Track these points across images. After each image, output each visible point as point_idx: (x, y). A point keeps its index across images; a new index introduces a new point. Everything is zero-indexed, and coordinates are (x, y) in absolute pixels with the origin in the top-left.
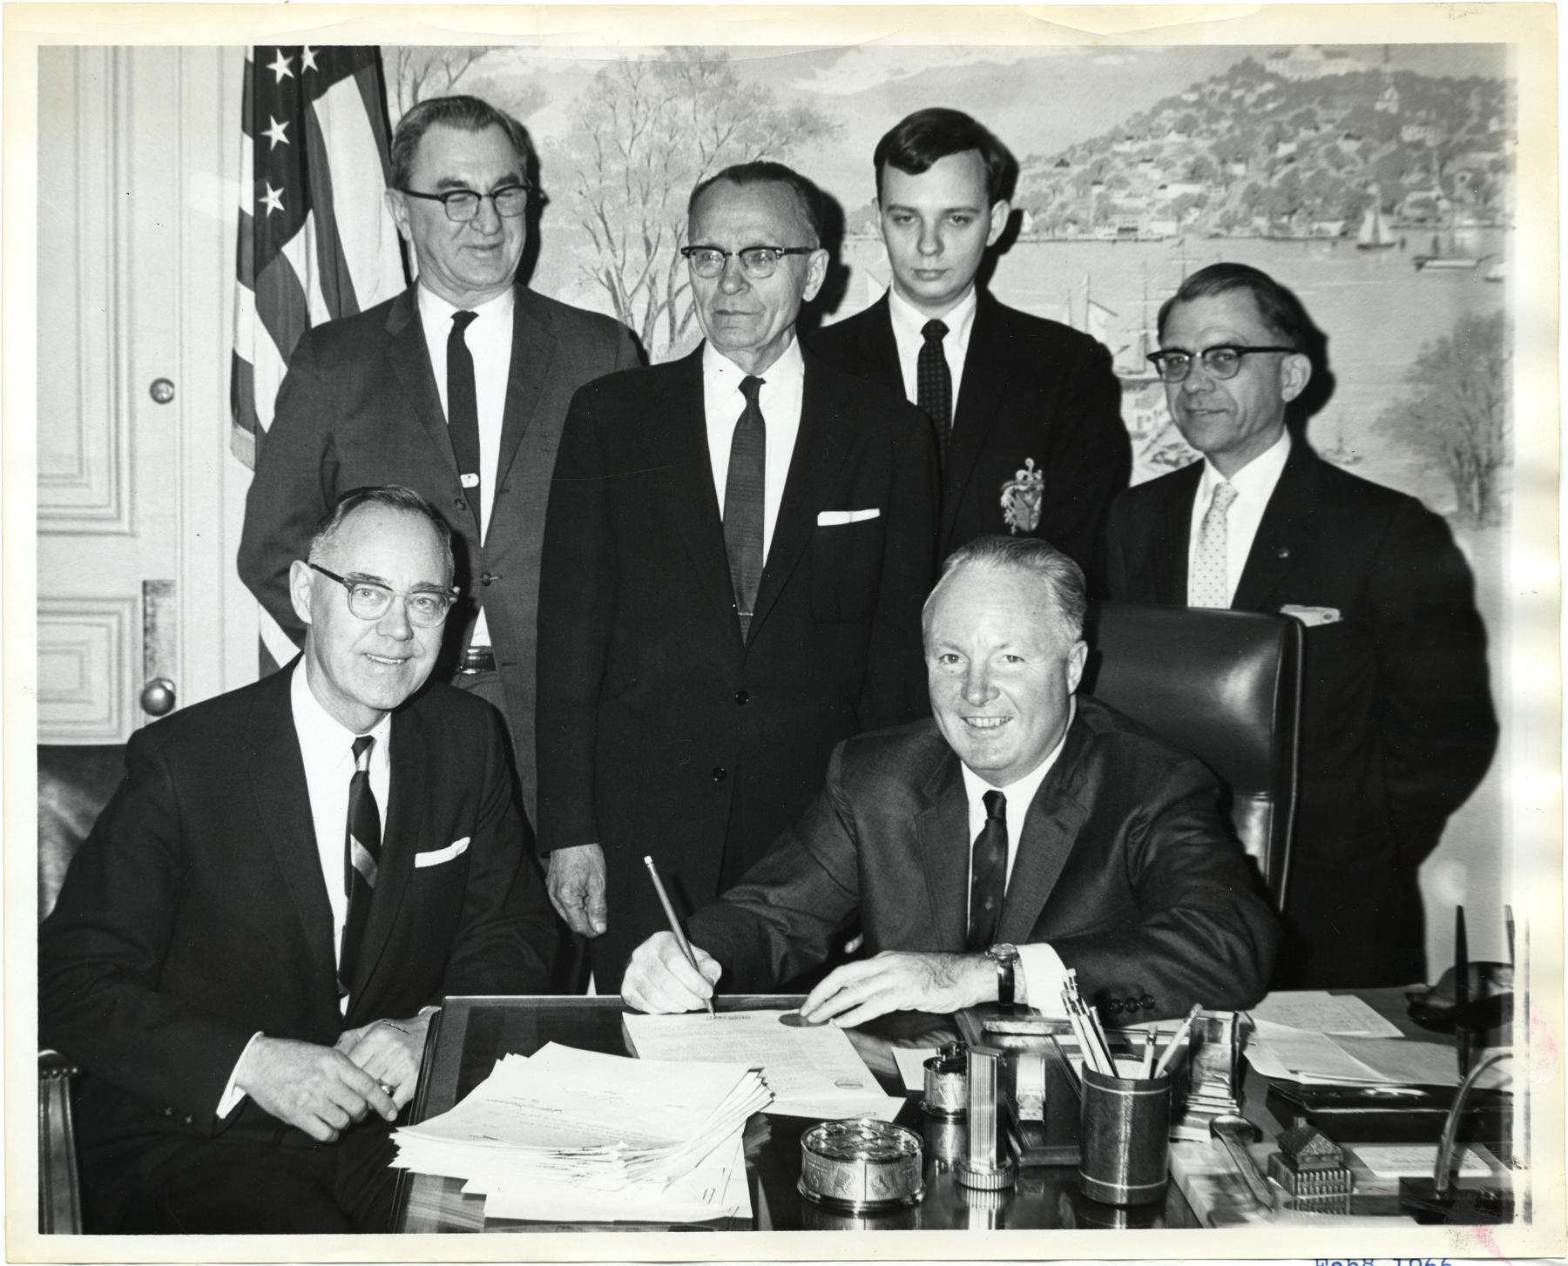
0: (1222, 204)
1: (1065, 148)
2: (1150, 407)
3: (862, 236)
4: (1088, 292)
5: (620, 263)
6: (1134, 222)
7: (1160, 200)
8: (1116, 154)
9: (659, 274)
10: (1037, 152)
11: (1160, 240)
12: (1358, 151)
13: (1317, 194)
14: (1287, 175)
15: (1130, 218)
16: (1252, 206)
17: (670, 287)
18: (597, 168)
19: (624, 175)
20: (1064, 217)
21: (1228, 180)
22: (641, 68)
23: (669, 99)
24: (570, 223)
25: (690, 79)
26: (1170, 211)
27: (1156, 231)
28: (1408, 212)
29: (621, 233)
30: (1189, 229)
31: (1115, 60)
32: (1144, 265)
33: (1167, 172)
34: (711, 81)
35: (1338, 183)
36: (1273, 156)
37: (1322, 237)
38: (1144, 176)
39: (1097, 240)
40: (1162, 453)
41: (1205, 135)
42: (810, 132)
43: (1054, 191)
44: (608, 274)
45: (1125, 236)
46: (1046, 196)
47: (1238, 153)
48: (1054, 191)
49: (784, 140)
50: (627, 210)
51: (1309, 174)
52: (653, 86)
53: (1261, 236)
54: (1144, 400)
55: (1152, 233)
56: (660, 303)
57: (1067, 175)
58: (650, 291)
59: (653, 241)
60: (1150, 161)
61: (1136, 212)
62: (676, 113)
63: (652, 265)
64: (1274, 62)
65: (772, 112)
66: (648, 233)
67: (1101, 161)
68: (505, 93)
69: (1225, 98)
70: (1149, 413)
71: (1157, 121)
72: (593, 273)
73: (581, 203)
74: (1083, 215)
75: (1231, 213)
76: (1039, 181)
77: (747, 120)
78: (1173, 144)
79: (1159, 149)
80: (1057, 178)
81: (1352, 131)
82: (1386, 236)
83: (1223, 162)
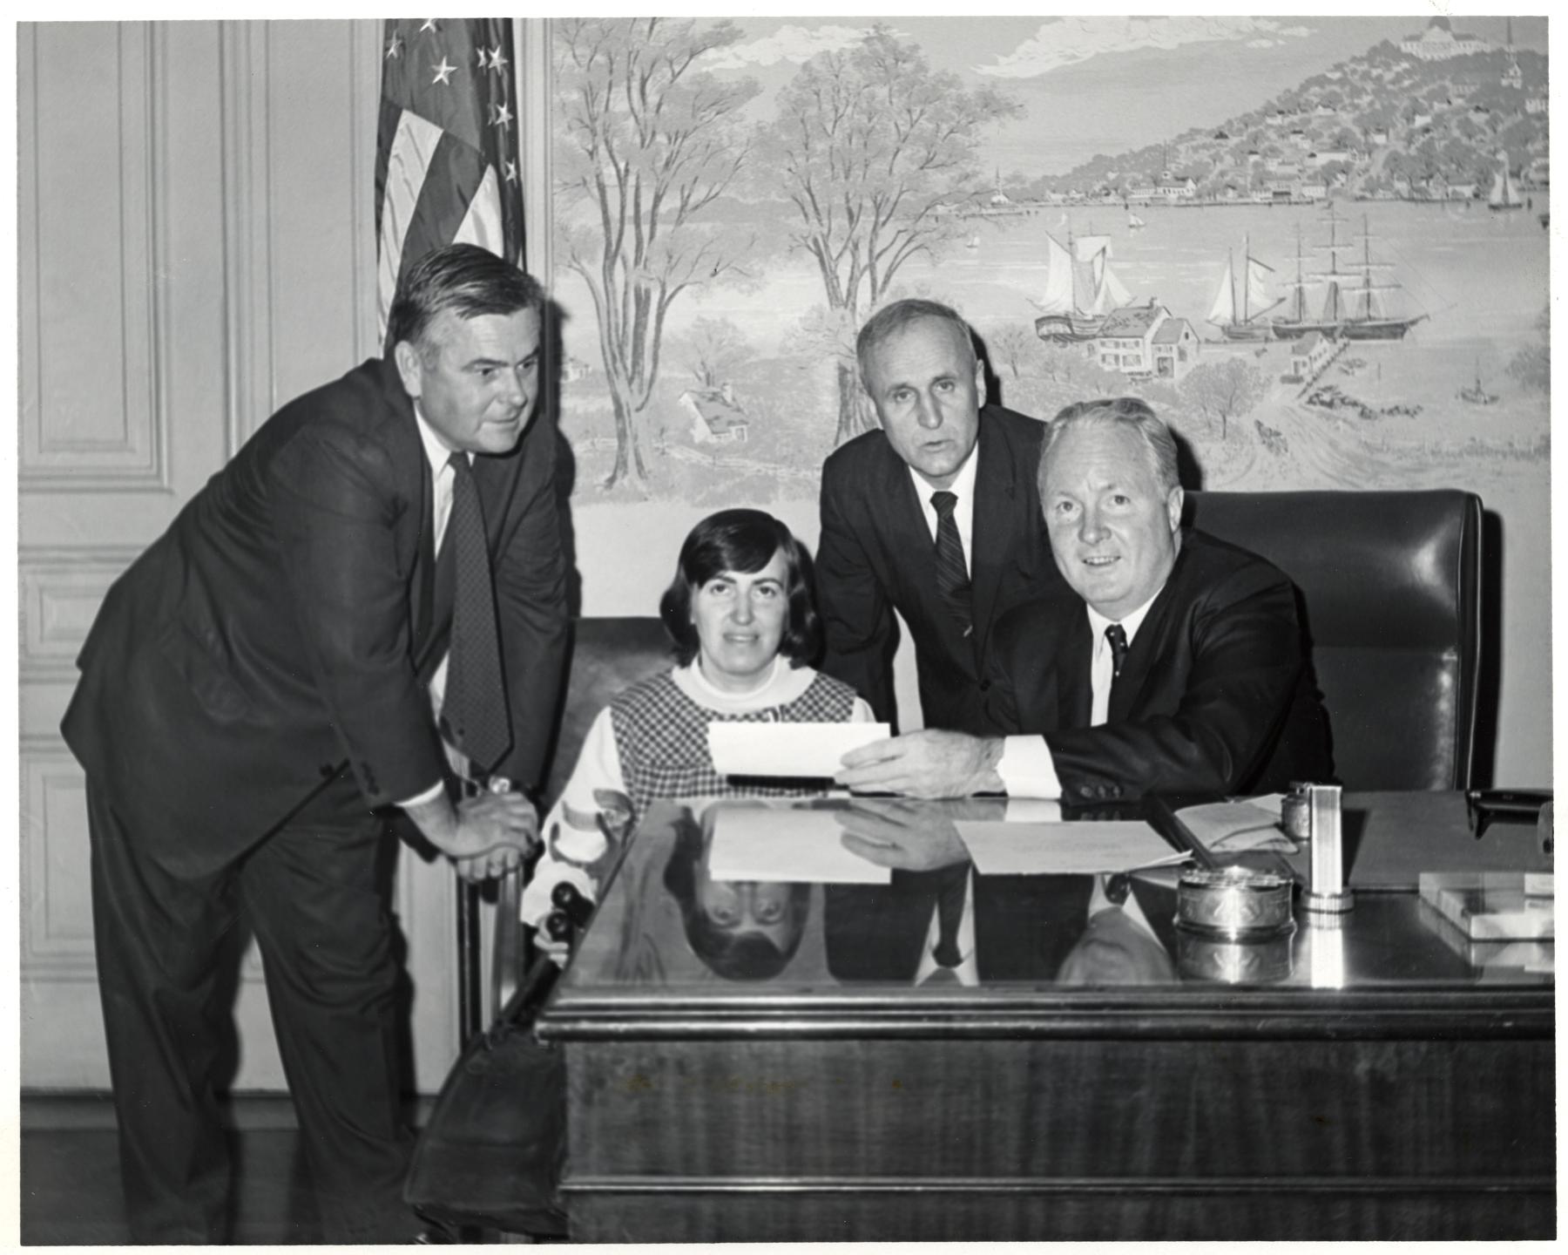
0: (1366, 170)
1: (1223, 123)
2: (1306, 353)
3: (1043, 203)
4: (1248, 251)
5: (825, 231)
6: (1288, 186)
7: (1309, 167)
8: (1271, 126)
9: (861, 240)
10: (1196, 127)
11: (1312, 202)
12: (1487, 122)
13: (1452, 161)
14: (1424, 143)
15: (1284, 183)
16: (1392, 172)
17: (871, 251)
18: (803, 147)
19: (828, 154)
20: (1224, 183)
21: (1370, 150)
22: (843, 59)
23: (867, 86)
24: (781, 197)
25: (886, 68)
26: (1319, 177)
27: (1307, 194)
28: (1533, 176)
29: (826, 205)
30: (1336, 192)
31: (1266, 44)
32: (1298, 225)
33: (1317, 141)
34: (904, 69)
35: (1470, 150)
36: (1411, 126)
37: (1457, 199)
38: (1296, 145)
39: (1255, 203)
40: (1317, 395)
41: (1349, 108)
42: (995, 112)
43: (1215, 161)
44: (816, 241)
45: (1280, 199)
46: (1208, 164)
47: (1379, 125)
48: (1215, 161)
49: (970, 119)
50: (832, 184)
51: (1443, 143)
52: (853, 75)
53: (1403, 199)
54: (1299, 346)
55: (1304, 196)
56: (862, 266)
57: (1226, 146)
58: (853, 255)
59: (855, 210)
60: (1300, 132)
61: (1290, 178)
62: (873, 98)
63: (855, 233)
64: (1409, 44)
65: (959, 95)
66: (851, 205)
67: (1256, 133)
68: (721, 84)
69: (1366, 76)
70: (1306, 359)
71: (1305, 95)
72: (802, 241)
73: (791, 179)
74: (1241, 181)
75: (1375, 177)
76: (1201, 151)
77: (937, 103)
78: (1320, 117)
79: (1309, 121)
80: (1218, 148)
81: (1481, 105)
82: (1514, 197)
83: (1366, 133)
